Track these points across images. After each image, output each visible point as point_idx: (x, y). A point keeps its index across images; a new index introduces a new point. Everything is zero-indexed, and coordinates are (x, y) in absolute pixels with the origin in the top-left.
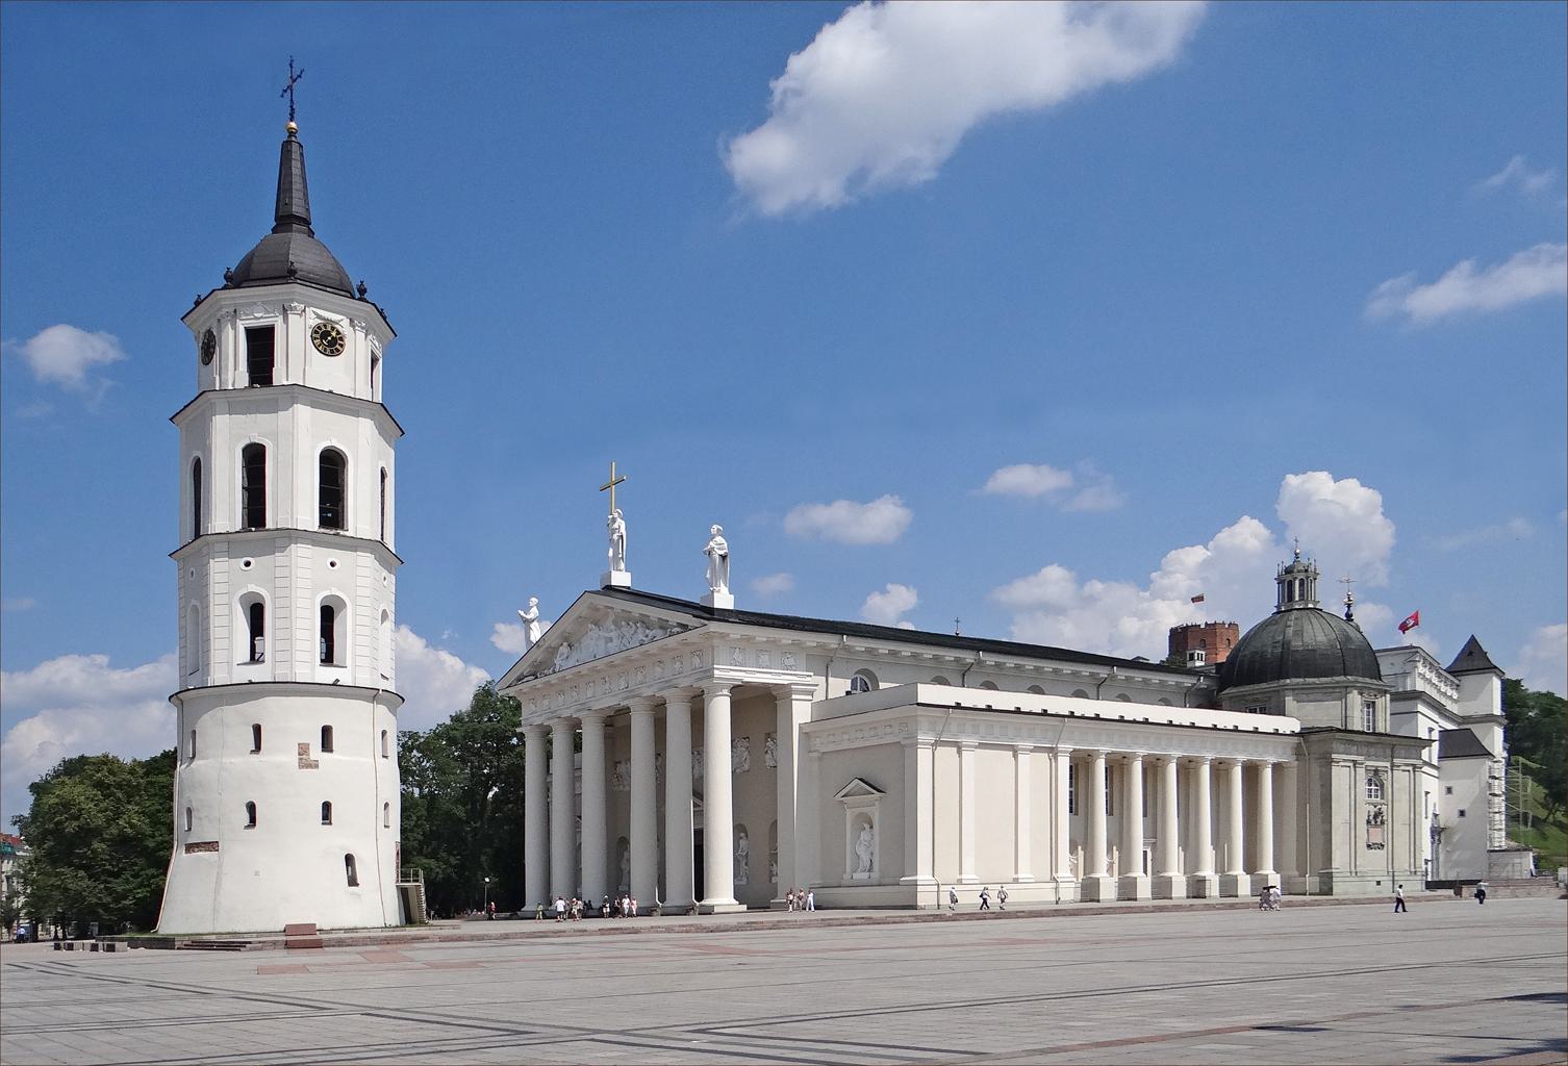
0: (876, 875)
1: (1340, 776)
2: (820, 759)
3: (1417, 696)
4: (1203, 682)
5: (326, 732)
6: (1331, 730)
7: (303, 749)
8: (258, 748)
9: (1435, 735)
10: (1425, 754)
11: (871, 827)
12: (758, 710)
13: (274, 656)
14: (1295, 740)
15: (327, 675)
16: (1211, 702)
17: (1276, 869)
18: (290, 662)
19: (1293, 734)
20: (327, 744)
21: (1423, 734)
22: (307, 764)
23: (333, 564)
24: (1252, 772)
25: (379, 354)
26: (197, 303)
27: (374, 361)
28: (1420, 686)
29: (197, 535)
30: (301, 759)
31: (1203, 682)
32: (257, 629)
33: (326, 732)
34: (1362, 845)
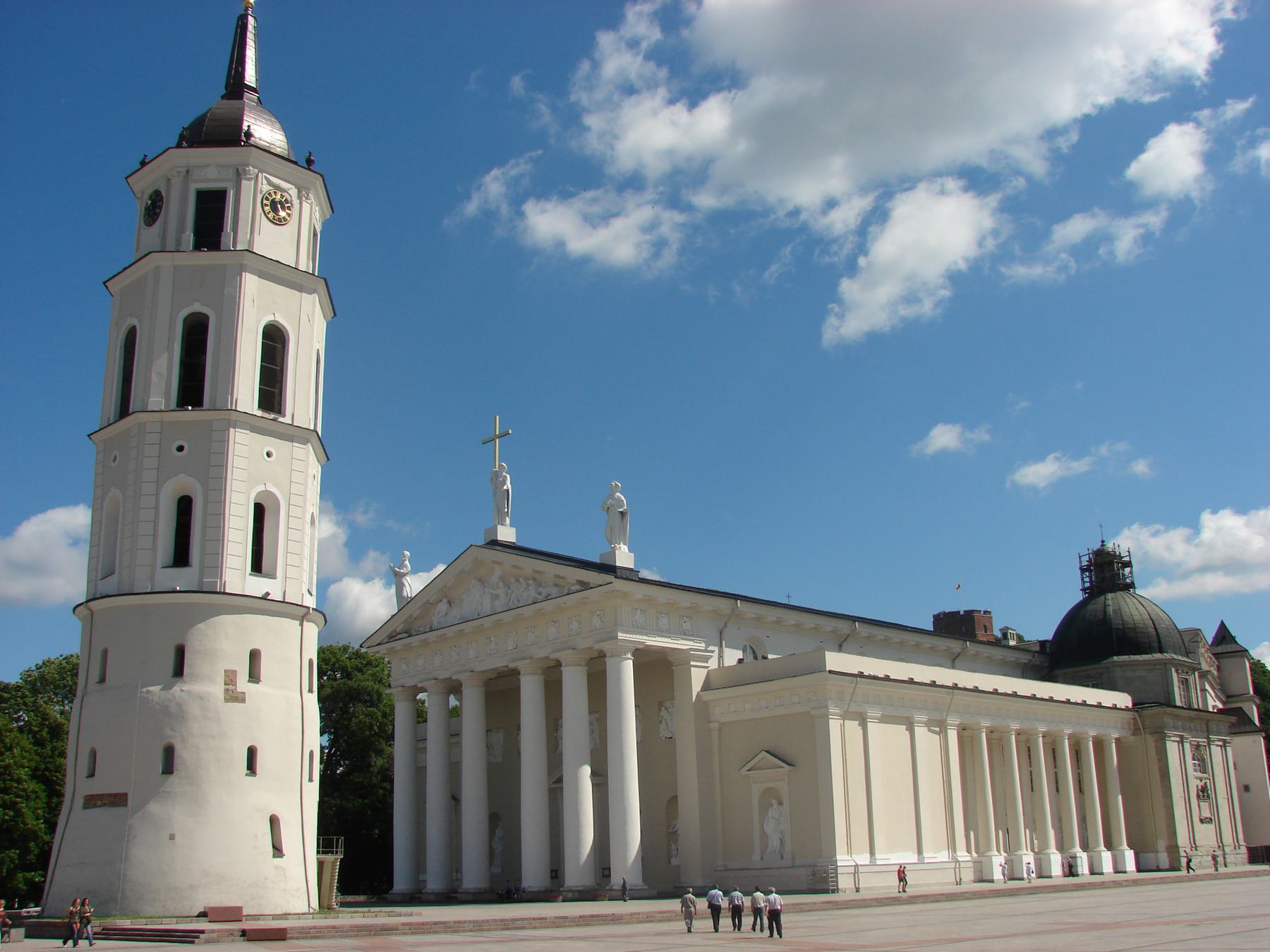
1: (1172, 748)
2: (720, 730)
5: (254, 656)
7: (230, 678)
8: (179, 671)
11: (780, 803)
12: (657, 672)
13: (202, 561)
14: (1130, 715)
19: (1127, 709)
22: (234, 697)
27: (315, 235)
30: (227, 690)
33: (254, 656)
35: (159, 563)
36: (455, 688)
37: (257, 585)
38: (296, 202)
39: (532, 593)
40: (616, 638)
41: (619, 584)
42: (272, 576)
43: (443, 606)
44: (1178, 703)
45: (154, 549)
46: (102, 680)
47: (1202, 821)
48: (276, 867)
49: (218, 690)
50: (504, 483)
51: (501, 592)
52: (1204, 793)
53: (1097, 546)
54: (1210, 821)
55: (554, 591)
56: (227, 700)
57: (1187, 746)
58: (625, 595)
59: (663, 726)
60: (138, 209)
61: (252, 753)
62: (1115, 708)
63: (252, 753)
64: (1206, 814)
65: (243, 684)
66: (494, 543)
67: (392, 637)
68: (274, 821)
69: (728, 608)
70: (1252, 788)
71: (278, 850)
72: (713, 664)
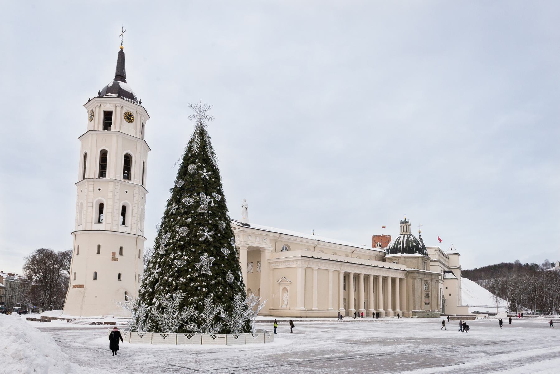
1: (417, 283)
5: (121, 248)
7: (114, 254)
15: (122, 229)
17: (401, 309)
23: (126, 192)
24: (393, 280)
26: (89, 101)
29: (84, 178)
32: (101, 211)
33: (121, 248)
34: (423, 303)
35: (94, 222)
45: (92, 218)
46: (78, 254)
56: (112, 260)
60: (87, 116)
61: (120, 275)
63: (120, 275)
65: (117, 255)
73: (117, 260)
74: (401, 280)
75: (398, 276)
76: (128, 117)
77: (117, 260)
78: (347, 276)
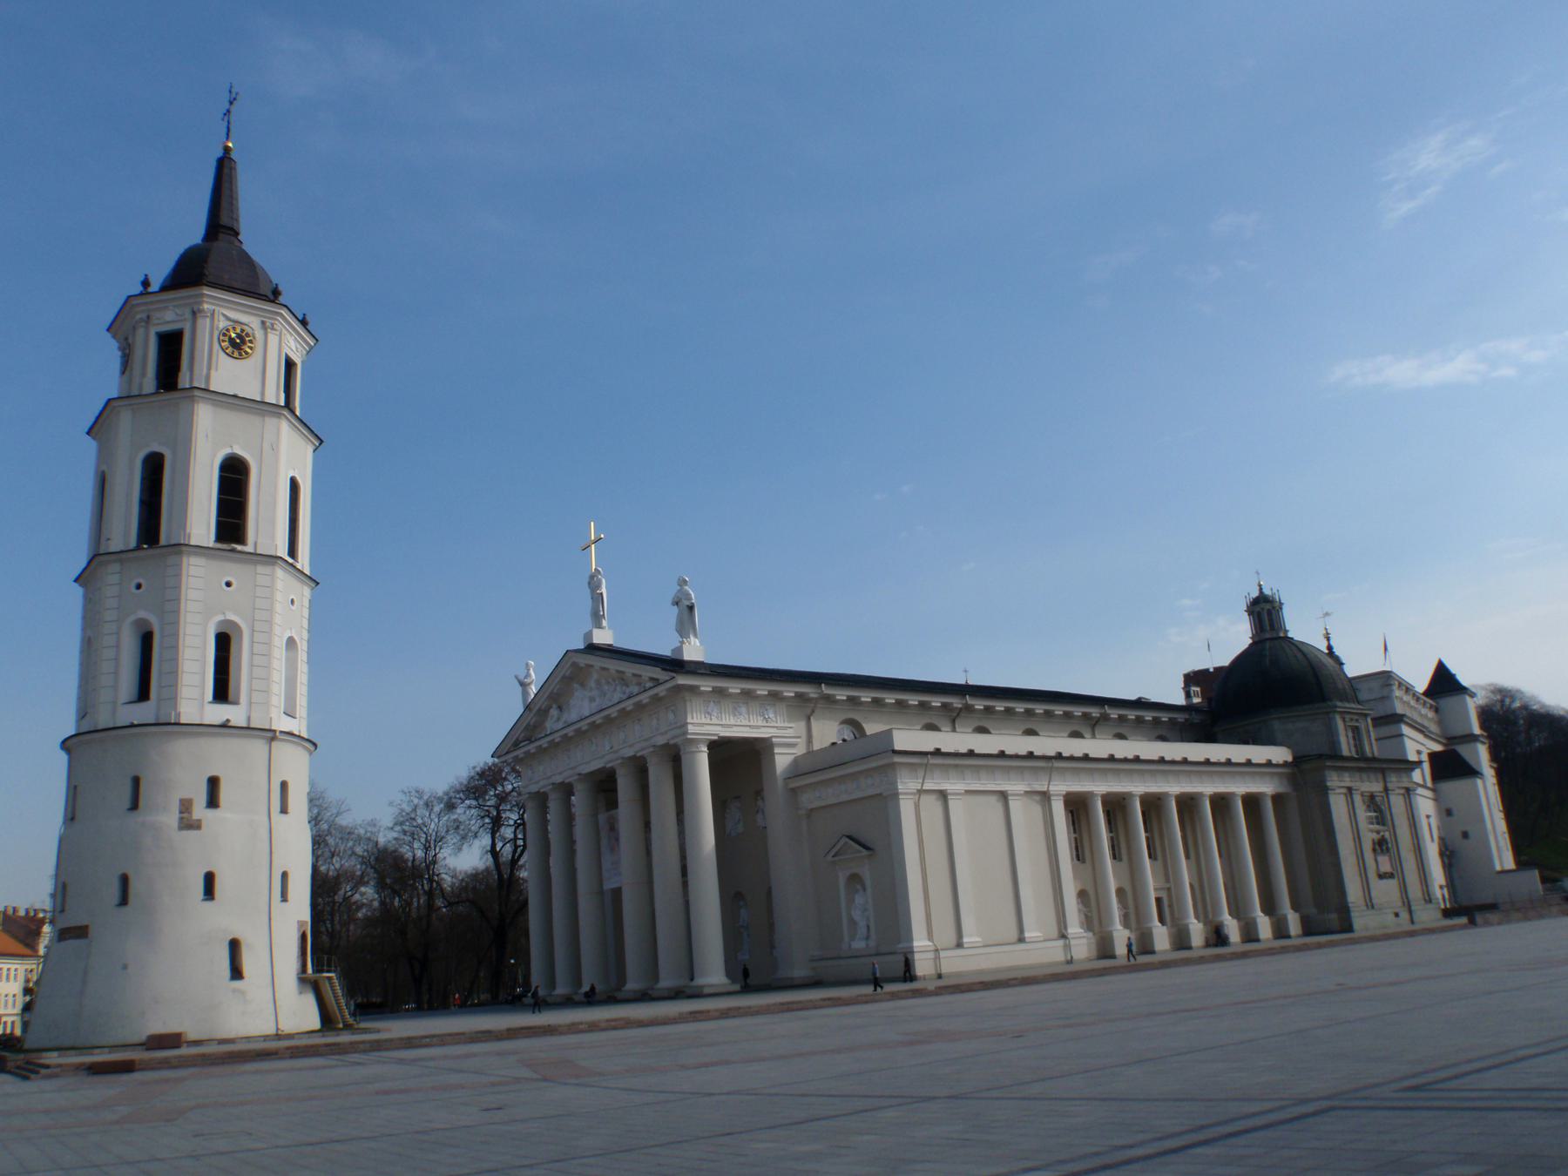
0: (872, 943)
3: (1397, 719)
4: (1196, 718)
5: (213, 783)
6: (1320, 756)
8: (135, 805)
9: (1425, 757)
10: (1417, 776)
16: (1206, 735)
18: (173, 699)
19: (1286, 764)
20: (213, 802)
21: (1412, 757)
22: (189, 824)
25: (297, 359)
27: (290, 365)
28: (1400, 709)
31: (1196, 718)
33: (213, 783)
36: (567, 790)
37: (219, 713)
38: (259, 334)
39: (617, 696)
40: (686, 733)
41: (682, 680)
42: (236, 703)
43: (554, 712)
44: (1345, 753)
47: (1381, 876)
48: (234, 991)
49: (171, 818)
50: (599, 586)
51: (595, 693)
52: (1381, 846)
53: (1255, 594)
54: (1391, 876)
55: (636, 689)
57: (1357, 798)
58: (693, 689)
59: (759, 816)
61: (209, 879)
62: (1269, 764)
63: (209, 879)
64: (1386, 866)
65: (200, 811)
66: (592, 649)
67: (516, 745)
68: (234, 946)
69: (809, 687)
70: (1471, 834)
71: (237, 973)
72: (800, 750)
73: (196, 826)
74: (1277, 799)
75: (1266, 787)
76: (231, 341)
77: (196, 826)
78: (1077, 807)
